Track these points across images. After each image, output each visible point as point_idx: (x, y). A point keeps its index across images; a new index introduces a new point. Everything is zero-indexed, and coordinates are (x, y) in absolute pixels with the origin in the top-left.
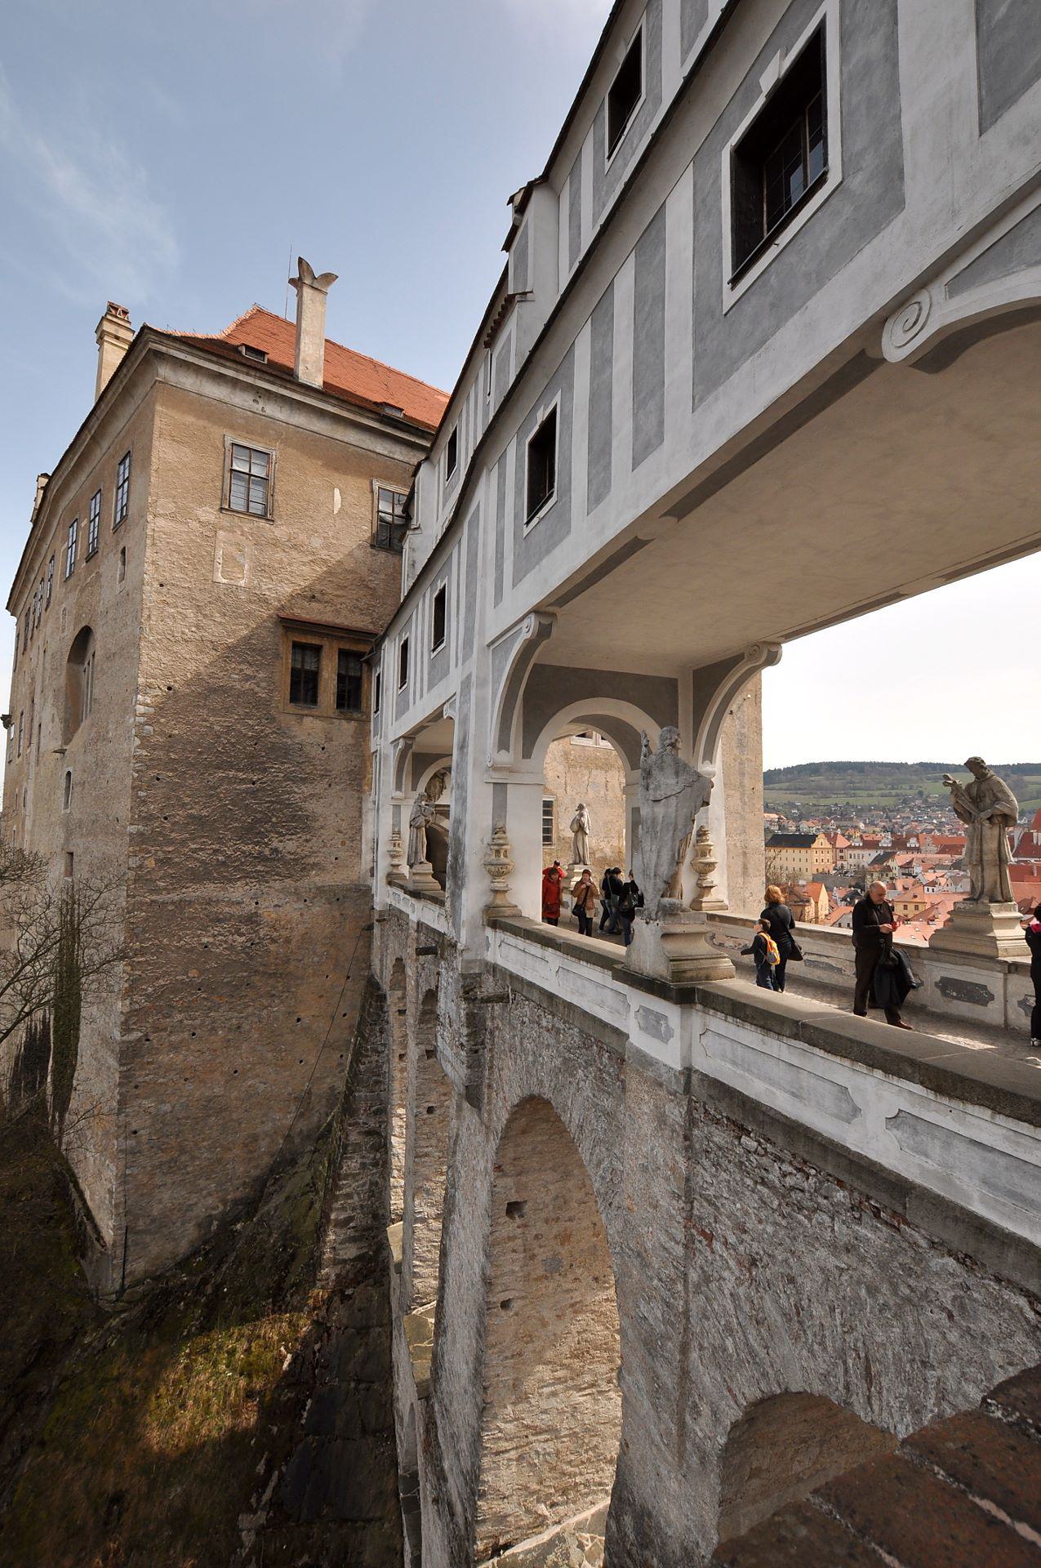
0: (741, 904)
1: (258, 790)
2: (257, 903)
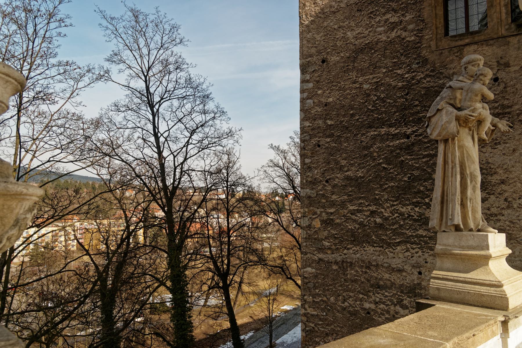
1: (413, 144)
2: (420, 273)
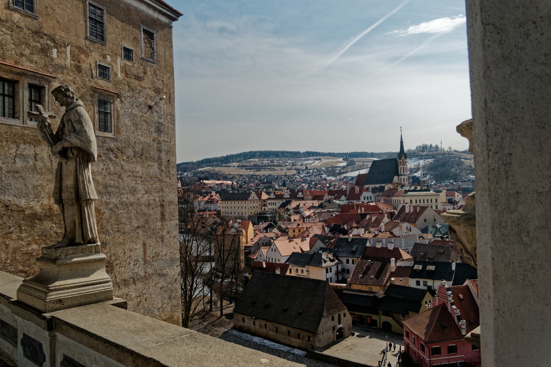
0: (159, 240)
